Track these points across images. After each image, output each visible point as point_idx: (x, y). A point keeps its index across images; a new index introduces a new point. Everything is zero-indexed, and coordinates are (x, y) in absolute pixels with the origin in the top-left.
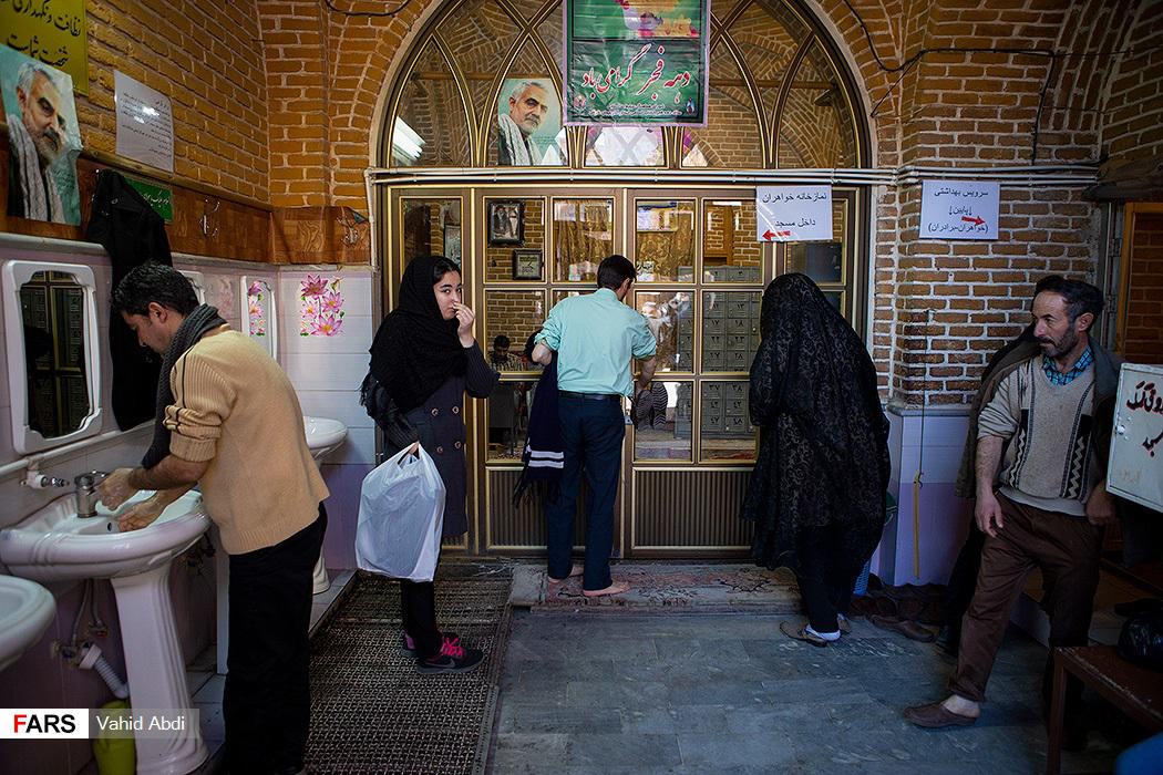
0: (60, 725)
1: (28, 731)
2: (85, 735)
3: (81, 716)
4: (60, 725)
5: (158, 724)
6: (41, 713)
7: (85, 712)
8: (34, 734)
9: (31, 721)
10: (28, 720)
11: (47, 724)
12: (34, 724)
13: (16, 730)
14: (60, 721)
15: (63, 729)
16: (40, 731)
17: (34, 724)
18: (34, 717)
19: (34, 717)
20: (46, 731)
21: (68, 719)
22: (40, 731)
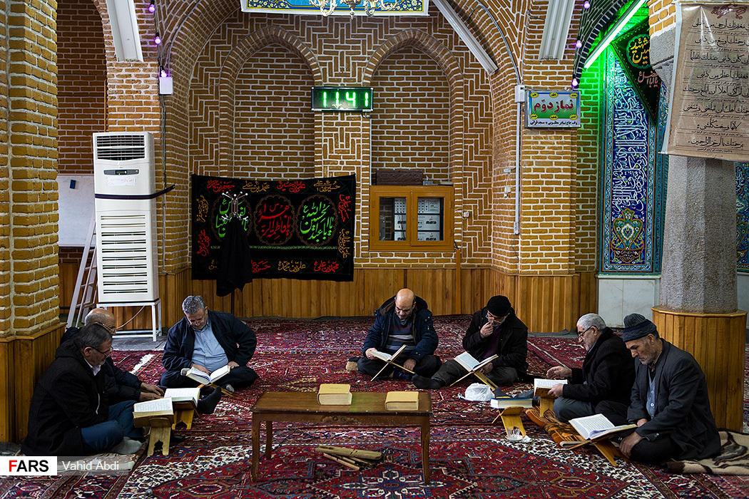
0: (39, 467)
1: (18, 470)
2: (55, 474)
3: (52, 461)
4: (39, 467)
6: (26, 459)
7: (55, 458)
8: (22, 473)
9: (20, 465)
10: (18, 464)
11: (30, 466)
12: (22, 466)
13: (10, 470)
14: (39, 464)
15: (41, 469)
16: (26, 471)
17: (22, 466)
18: (22, 462)
19: (22, 462)
20: (30, 470)
21: (44, 463)
22: (26, 471)
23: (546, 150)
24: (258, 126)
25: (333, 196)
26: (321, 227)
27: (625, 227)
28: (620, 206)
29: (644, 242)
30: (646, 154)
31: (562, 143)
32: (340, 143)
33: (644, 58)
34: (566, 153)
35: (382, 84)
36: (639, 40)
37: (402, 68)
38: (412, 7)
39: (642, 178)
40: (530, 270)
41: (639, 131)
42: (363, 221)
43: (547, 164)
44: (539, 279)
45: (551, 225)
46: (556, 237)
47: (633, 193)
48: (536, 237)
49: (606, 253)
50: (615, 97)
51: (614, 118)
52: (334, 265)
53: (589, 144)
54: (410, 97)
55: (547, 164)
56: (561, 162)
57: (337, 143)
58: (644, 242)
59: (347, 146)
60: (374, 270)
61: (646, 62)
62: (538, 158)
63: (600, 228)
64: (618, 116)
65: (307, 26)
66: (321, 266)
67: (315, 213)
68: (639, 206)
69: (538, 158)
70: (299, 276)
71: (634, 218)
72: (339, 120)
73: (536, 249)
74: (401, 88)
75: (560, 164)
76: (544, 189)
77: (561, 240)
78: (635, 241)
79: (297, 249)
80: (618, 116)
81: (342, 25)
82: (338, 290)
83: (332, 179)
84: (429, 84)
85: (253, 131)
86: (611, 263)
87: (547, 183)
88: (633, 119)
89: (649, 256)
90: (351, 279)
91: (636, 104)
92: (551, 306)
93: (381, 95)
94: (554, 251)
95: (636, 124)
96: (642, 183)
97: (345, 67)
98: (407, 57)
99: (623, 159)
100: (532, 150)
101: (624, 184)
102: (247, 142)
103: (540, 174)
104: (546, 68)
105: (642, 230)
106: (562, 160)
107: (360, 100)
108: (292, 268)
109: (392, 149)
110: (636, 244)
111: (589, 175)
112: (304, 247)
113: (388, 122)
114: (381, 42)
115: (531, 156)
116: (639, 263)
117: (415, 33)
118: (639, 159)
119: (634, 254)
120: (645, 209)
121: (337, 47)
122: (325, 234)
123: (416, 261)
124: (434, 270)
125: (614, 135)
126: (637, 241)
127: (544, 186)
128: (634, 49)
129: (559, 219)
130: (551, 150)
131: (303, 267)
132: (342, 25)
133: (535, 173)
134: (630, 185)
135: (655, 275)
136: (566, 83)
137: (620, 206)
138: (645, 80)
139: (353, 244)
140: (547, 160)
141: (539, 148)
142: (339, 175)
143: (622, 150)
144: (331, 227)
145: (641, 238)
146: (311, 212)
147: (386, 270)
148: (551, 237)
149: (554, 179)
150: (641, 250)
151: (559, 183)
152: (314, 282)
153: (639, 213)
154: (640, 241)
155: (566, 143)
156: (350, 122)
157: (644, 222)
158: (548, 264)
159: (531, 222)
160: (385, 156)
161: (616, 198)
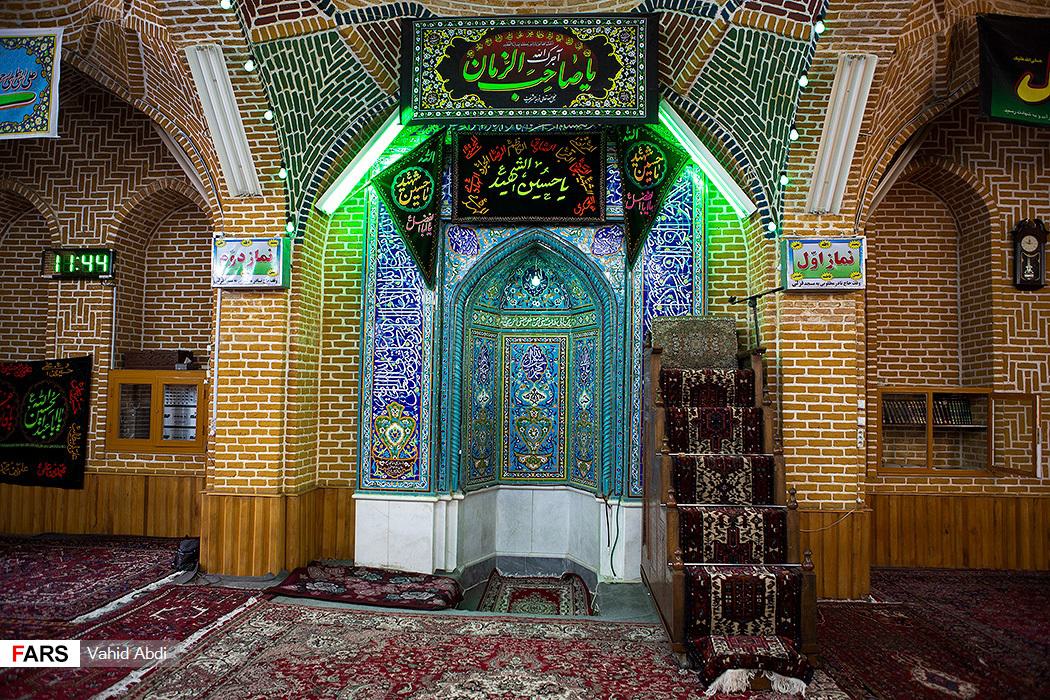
0: (54, 655)
1: (25, 660)
2: (77, 664)
3: (73, 647)
4: (54, 655)
5: (142, 654)
6: (37, 644)
7: (78, 643)
8: (31, 663)
9: (28, 652)
10: (25, 650)
11: (42, 654)
12: (31, 654)
13: (15, 660)
14: (54, 651)
15: (57, 658)
16: (36, 660)
17: (31, 654)
18: (31, 648)
19: (31, 648)
20: (42, 660)
21: (61, 650)
22: (36, 660)
23: (250, 319)
24: (22, 299)
25: (62, 384)
26: (48, 421)
27: (392, 427)
28: (384, 398)
29: (418, 449)
30: (421, 327)
31: (271, 310)
32: (78, 317)
33: (415, 198)
34: (277, 324)
35: (162, 249)
36: (408, 174)
37: (186, 229)
38: (36, 127)
39: (415, 361)
40: (225, 486)
41: (410, 295)
42: (100, 413)
43: (249, 339)
44: (234, 501)
45: (254, 424)
46: (261, 441)
47: (402, 381)
48: (234, 441)
49: (366, 463)
50: (379, 251)
51: (378, 278)
52: (61, 468)
53: (352, 314)
54: (194, 264)
55: (249, 339)
56: (269, 336)
57: (73, 316)
58: (418, 449)
59: (86, 321)
60: (109, 474)
61: (418, 203)
62: (240, 330)
63: (358, 428)
64: (382, 276)
65: (48, 179)
66: (47, 470)
67: (42, 403)
68: (411, 399)
69: (240, 330)
70: (24, 480)
71: (403, 415)
72: (78, 290)
73: (234, 457)
74: (184, 253)
75: (268, 338)
76: (246, 373)
77: (268, 445)
78: (406, 448)
79: (24, 448)
80: (382, 276)
81: (88, 176)
82: (65, 500)
83: (64, 362)
84: (198, 248)
85: (16, 305)
86: (372, 477)
87: (250, 365)
88: (402, 280)
89: (424, 468)
90: (79, 485)
91: (407, 259)
92: (250, 538)
93: (161, 262)
94: (258, 461)
95: (407, 286)
96: (414, 366)
97: (88, 226)
98: (192, 216)
99: (388, 334)
100: (232, 320)
101: (389, 368)
102: (9, 318)
103: (241, 352)
104: (250, 209)
105: (414, 432)
106: (271, 334)
107: (64, 264)
108: (12, 472)
109: (170, 326)
110: (406, 452)
111: (352, 357)
112: (27, 445)
113: (167, 294)
114: (131, 195)
115: (230, 327)
116: (411, 478)
117: (169, 183)
118: (410, 334)
119: (404, 466)
120: (418, 404)
121: (81, 202)
122: (52, 429)
123: (162, 465)
124: (181, 478)
125: (377, 302)
126: (408, 447)
127: (246, 369)
128: (402, 187)
129: (265, 415)
130: (257, 320)
131: (25, 469)
132: (88, 176)
133: (234, 352)
134: (398, 370)
135: (432, 495)
136: (278, 229)
137: (384, 398)
138: (416, 226)
139: (86, 443)
140: (252, 333)
141: (241, 317)
142: (75, 356)
143: (387, 322)
144: (59, 421)
145: (414, 442)
146: (38, 401)
147: (124, 476)
148: (253, 440)
149: (259, 360)
150: (413, 460)
151: (266, 365)
152: (38, 489)
153: (411, 409)
154: (412, 447)
155: (277, 310)
156: (90, 291)
157: (418, 422)
158: (249, 479)
159: (227, 419)
160: (162, 335)
161: (379, 387)
